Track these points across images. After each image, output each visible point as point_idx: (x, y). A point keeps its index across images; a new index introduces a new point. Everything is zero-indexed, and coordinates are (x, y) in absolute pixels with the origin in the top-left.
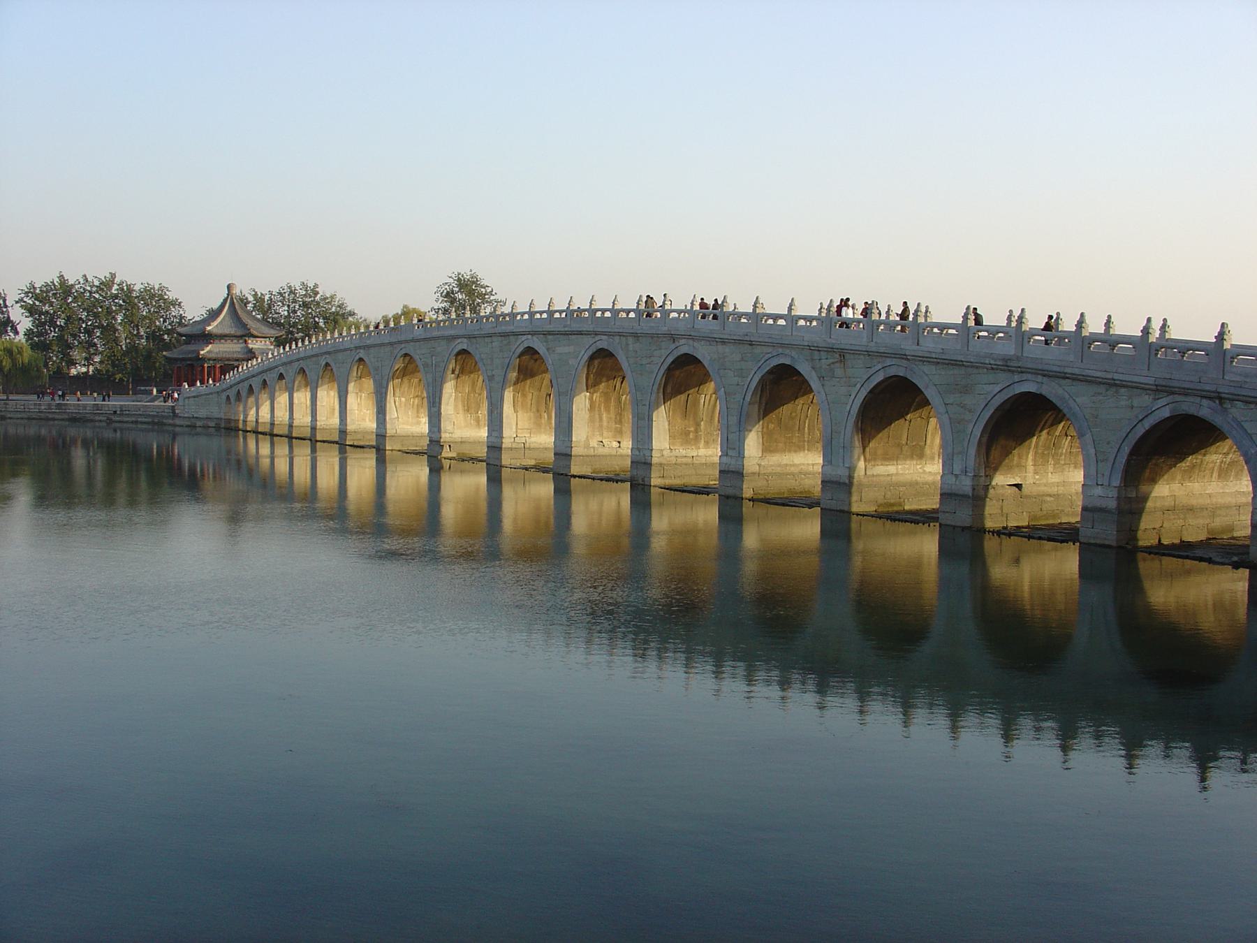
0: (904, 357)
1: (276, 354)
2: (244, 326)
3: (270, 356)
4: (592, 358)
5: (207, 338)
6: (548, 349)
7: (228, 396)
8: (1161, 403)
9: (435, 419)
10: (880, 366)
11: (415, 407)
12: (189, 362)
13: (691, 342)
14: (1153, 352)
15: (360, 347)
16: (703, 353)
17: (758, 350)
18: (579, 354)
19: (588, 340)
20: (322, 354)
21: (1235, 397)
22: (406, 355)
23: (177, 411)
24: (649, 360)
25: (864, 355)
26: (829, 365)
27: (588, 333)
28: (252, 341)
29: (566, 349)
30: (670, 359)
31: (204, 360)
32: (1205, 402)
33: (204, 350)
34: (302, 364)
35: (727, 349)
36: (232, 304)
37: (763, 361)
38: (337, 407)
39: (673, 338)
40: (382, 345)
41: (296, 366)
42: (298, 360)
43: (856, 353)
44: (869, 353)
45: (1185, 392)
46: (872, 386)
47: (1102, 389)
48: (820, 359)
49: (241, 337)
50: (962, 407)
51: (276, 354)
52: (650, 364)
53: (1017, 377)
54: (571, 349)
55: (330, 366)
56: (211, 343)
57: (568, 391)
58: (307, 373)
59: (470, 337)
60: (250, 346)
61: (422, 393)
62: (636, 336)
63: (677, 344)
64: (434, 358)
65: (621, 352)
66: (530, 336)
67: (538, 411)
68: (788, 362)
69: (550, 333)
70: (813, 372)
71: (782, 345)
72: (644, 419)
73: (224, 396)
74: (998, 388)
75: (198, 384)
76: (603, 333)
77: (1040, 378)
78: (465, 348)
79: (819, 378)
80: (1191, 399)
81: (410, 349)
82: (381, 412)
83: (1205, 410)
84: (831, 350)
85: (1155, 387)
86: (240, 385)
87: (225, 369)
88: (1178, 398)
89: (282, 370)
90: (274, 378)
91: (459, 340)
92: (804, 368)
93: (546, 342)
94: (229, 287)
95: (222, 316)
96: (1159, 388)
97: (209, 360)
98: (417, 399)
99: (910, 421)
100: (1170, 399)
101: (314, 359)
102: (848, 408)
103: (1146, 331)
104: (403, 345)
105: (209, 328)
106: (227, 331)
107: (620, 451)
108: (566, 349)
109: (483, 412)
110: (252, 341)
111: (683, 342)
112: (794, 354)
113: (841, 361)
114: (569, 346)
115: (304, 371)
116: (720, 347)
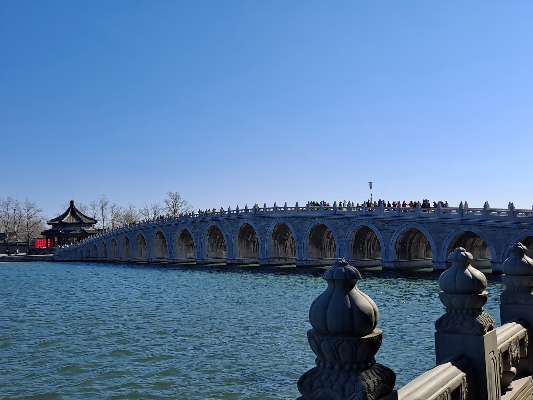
8: (520, 232)
15: (158, 227)
18: (270, 225)
24: (302, 227)
29: (264, 223)
50: (440, 238)
64: (198, 229)
67: (247, 248)
88: (526, 230)
91: (211, 222)
102: (391, 241)
103: (461, 204)
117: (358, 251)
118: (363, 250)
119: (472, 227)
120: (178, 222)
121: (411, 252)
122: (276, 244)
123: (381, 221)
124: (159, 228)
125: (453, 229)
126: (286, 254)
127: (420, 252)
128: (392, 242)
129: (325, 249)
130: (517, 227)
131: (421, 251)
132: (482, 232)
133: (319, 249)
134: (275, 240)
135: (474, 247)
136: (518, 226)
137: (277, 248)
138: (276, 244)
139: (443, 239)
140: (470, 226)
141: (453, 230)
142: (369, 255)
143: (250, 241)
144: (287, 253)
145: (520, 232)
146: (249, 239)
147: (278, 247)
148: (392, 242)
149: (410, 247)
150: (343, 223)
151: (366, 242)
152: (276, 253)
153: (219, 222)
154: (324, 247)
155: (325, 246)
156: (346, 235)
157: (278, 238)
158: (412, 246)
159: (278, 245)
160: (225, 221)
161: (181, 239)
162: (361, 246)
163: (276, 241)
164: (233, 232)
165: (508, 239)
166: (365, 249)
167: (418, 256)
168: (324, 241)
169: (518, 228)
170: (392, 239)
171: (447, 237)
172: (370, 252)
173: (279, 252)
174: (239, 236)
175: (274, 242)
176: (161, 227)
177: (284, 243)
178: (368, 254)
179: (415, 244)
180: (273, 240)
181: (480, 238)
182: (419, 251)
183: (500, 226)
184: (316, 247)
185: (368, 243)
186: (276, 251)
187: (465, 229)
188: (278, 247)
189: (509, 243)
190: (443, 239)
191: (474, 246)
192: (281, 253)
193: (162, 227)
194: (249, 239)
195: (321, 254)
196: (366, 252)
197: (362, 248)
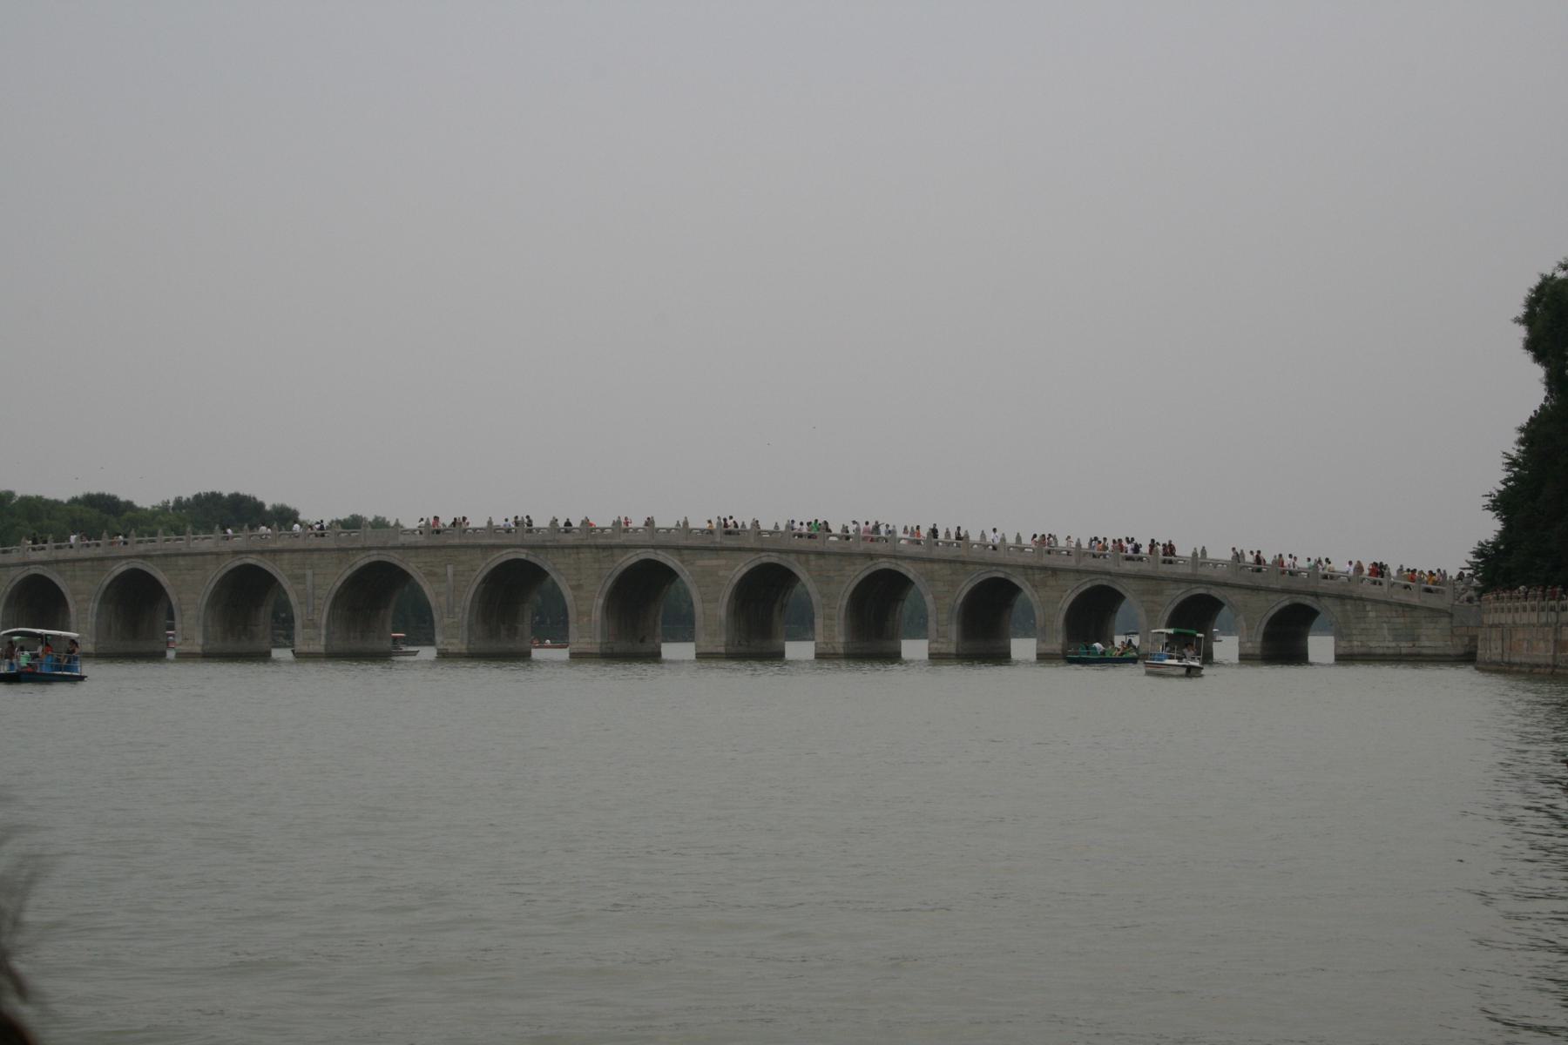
6: (682, 562)
10: (1087, 579)
13: (894, 561)
17: (970, 567)
19: (753, 556)
27: (751, 550)
35: (936, 567)
39: (870, 556)
44: (1078, 571)
53: (1193, 586)
63: (875, 561)
66: (652, 550)
69: (687, 548)
71: (994, 564)
76: (773, 551)
77: (1209, 586)
84: (1044, 569)
108: (715, 562)
111: (881, 560)
112: (1008, 570)
116: (928, 566)
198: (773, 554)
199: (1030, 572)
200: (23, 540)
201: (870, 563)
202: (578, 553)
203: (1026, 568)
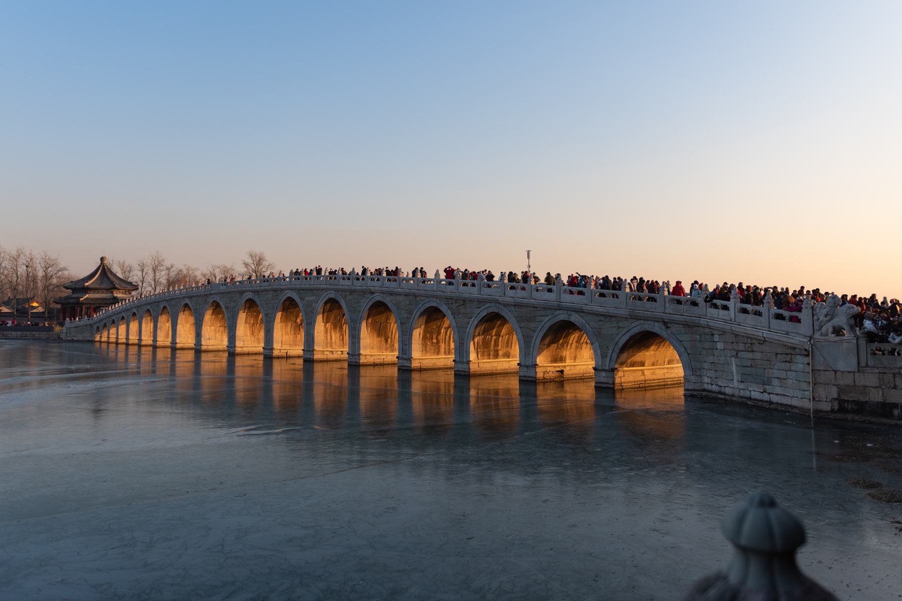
0: (497, 302)
1: (131, 300)
2: (112, 283)
3: (127, 301)
4: (326, 303)
5: (86, 290)
6: (300, 298)
7: (98, 326)
8: (633, 325)
9: (232, 338)
10: (485, 307)
11: (220, 331)
12: (73, 305)
14: (628, 297)
16: (388, 300)
18: (318, 301)
20: (162, 301)
21: (672, 321)
22: (214, 301)
23: (61, 336)
25: (476, 301)
26: (458, 306)
28: (117, 292)
30: (370, 304)
31: (82, 303)
32: (656, 324)
33: (82, 298)
34: (149, 307)
36: (104, 269)
37: (421, 305)
38: (170, 333)
40: (200, 296)
41: (145, 309)
42: (146, 304)
43: (471, 300)
45: (646, 319)
46: (480, 318)
47: (603, 318)
48: (452, 304)
49: (109, 289)
51: (131, 300)
52: (358, 306)
54: (314, 298)
55: (166, 308)
56: (88, 293)
57: (311, 323)
58: (152, 313)
59: (253, 291)
60: (115, 295)
61: (225, 324)
62: (352, 292)
63: (374, 295)
65: (342, 300)
66: (290, 291)
67: (295, 334)
68: (435, 305)
70: (449, 311)
72: (355, 338)
73: (95, 327)
74: (547, 318)
75: (77, 319)
78: (251, 298)
79: (452, 314)
80: (649, 322)
81: (217, 298)
82: (198, 335)
83: (657, 328)
84: (457, 300)
85: (630, 317)
86: (107, 320)
87: (97, 309)
88: (642, 322)
89: (135, 310)
90: (129, 315)
91: (248, 293)
92: (444, 308)
93: (300, 294)
94: (102, 259)
95: (96, 277)
96: (633, 317)
97: (86, 304)
98: (221, 328)
99: (502, 337)
100: (638, 322)
101: (156, 304)
104: (213, 296)
105: (86, 284)
106: (97, 286)
107: (343, 356)
109: (262, 334)
110: (117, 292)
113: (464, 304)
114: (312, 296)
115: (149, 311)
117: (429, 344)
118: (438, 342)
119: (571, 315)
120: (208, 292)
121: (499, 348)
122: (329, 329)
123: (456, 301)
124: (187, 299)
125: (547, 316)
126: (343, 343)
127: (513, 347)
128: (469, 333)
129: (393, 339)
130: (630, 317)
131: (515, 346)
132: (585, 322)
133: (383, 339)
134: (326, 323)
135: (583, 343)
136: (631, 316)
137: (329, 334)
138: (329, 329)
139: (533, 331)
140: (569, 313)
141: (547, 318)
142: (447, 350)
143: (299, 323)
144: (345, 343)
145: (633, 325)
146: (299, 321)
147: (331, 334)
148: (469, 333)
149: (496, 342)
150: (408, 302)
151: (443, 330)
152: (327, 342)
153: (256, 293)
154: (390, 336)
155: (392, 335)
156: (412, 319)
157: (331, 320)
158: (500, 339)
159: (331, 331)
160: (264, 293)
161: (213, 316)
162: (434, 336)
163: (328, 325)
164: (274, 309)
165: (618, 334)
166: (441, 342)
167: (510, 353)
168: (391, 327)
169: (632, 318)
170: (469, 327)
171: (538, 329)
172: (449, 345)
173: (332, 341)
174: (282, 315)
175: (325, 326)
176: (189, 298)
177: (341, 328)
178: (445, 349)
179: (504, 336)
180: (324, 324)
181: (583, 332)
182: (511, 347)
183: (608, 314)
184: (379, 335)
185: (446, 333)
186: (327, 339)
187: (562, 316)
188: (331, 334)
189: (619, 340)
190: (534, 331)
191: (582, 342)
192: (335, 343)
193: (190, 297)
194: (299, 321)
195: (386, 345)
196: (442, 345)
197: (437, 338)
198: (332, 291)
199: (450, 301)
200: (147, 290)
201: (371, 297)
202: (267, 294)
203: (449, 300)
